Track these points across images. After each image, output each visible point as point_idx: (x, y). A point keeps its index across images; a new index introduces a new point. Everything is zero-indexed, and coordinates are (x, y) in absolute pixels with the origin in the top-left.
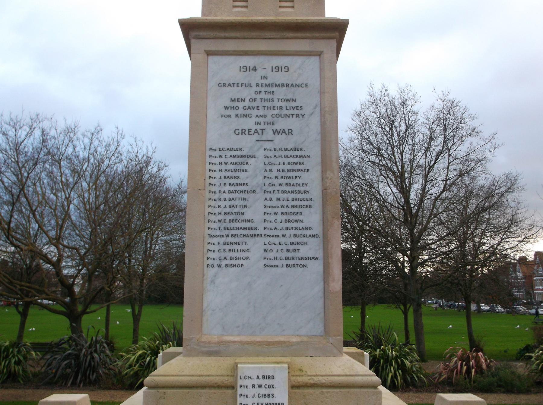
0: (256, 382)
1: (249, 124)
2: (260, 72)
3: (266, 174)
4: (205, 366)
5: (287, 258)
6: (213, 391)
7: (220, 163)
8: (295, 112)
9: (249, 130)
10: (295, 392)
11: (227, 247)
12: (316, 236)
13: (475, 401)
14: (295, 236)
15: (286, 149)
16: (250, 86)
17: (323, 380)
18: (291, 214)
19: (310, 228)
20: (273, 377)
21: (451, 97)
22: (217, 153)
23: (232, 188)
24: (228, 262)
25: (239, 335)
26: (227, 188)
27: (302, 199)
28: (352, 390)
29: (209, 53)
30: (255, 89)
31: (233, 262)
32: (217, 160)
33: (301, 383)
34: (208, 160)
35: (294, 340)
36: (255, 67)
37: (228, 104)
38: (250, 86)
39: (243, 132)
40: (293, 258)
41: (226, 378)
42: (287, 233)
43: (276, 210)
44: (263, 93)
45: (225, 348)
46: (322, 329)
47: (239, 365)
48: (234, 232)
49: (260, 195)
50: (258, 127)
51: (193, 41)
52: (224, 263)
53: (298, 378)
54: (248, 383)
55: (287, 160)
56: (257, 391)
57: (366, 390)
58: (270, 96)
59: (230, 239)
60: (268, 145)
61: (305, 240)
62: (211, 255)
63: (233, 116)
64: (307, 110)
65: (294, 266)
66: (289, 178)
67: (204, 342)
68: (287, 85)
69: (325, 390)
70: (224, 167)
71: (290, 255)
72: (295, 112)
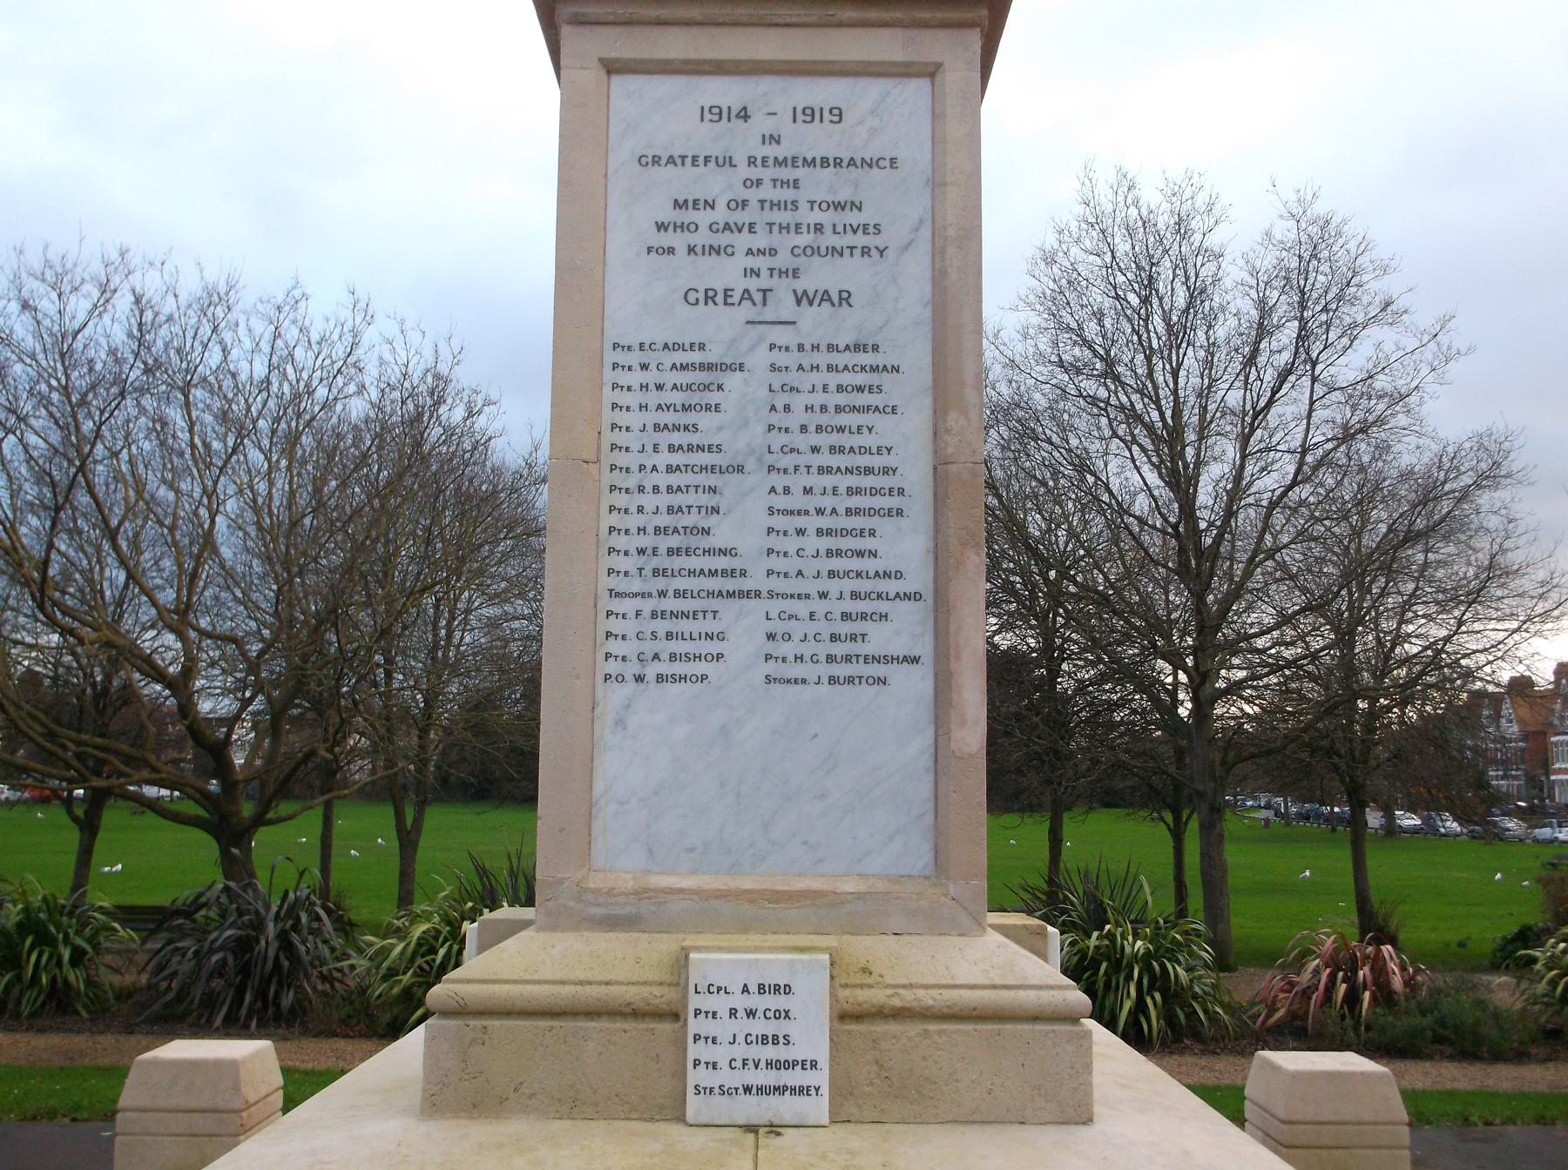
0: (741, 1002)
1: (728, 273)
2: (760, 124)
3: (775, 419)
4: (599, 957)
5: (831, 659)
6: (619, 1025)
7: (644, 387)
8: (860, 240)
9: (727, 293)
10: (849, 1032)
11: (661, 626)
12: (916, 596)
13: (1362, 1073)
14: (855, 595)
15: (831, 348)
16: (730, 162)
17: (928, 998)
18: (845, 533)
19: (899, 575)
20: (788, 990)
21: (1319, 209)
22: (634, 358)
23: (678, 459)
24: (665, 668)
25: (694, 872)
26: (663, 459)
27: (874, 492)
28: (1008, 1026)
29: (612, 68)
30: (744, 171)
31: (679, 668)
32: (636, 378)
33: (865, 1006)
34: (609, 376)
35: (850, 886)
37: (668, 214)
38: (730, 162)
39: (710, 297)
40: (848, 659)
41: (657, 991)
42: (833, 586)
43: (800, 522)
44: (767, 184)
45: (653, 908)
46: (929, 857)
47: (692, 956)
48: (681, 583)
49: (756, 479)
50: (753, 284)
51: (566, 32)
52: (652, 670)
53: (858, 991)
54: (719, 1003)
55: (834, 380)
56: (743, 1026)
57: (1048, 1027)
58: (787, 194)
59: (670, 604)
60: (782, 336)
61: (883, 606)
62: (616, 647)
63: (681, 250)
64: (892, 236)
65: (850, 680)
66: (841, 430)
67: (595, 891)
68: (838, 163)
69: (933, 1027)
70: (653, 398)
71: (839, 649)
72: (860, 240)
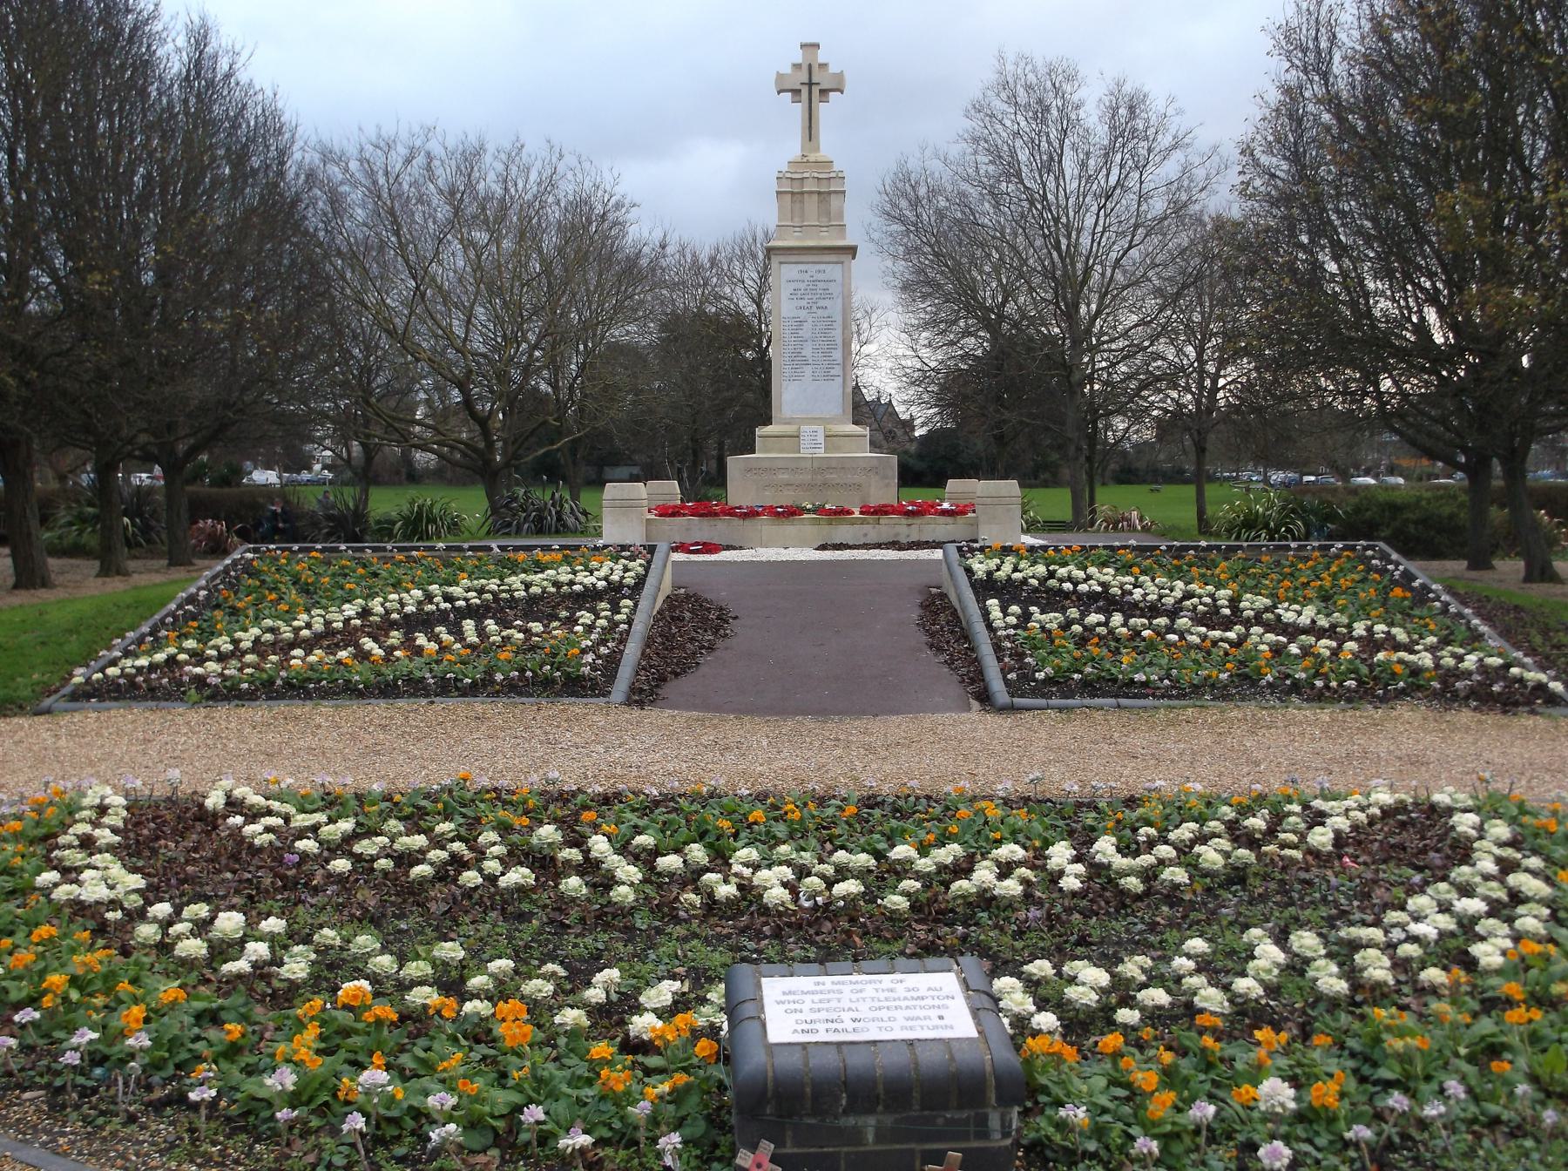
1: (804, 303)
36: (803, 46)
